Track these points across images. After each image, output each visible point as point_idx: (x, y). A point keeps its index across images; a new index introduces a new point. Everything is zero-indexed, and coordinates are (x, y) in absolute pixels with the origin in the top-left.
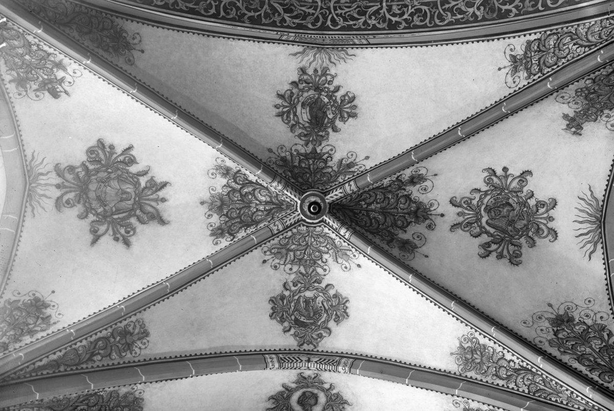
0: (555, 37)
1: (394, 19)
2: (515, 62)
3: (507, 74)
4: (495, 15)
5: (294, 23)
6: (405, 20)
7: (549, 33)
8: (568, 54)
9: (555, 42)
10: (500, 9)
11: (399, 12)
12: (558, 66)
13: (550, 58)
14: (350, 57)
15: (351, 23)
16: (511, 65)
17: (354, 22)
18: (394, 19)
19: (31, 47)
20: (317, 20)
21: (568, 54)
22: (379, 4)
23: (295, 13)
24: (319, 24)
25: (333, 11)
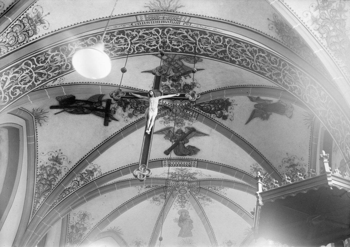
0: (19, 41)
1: (122, 36)
2: (40, 21)
3: (43, 12)
4: (61, 48)
5: (181, 30)
6: (115, 36)
7: (25, 42)
8: (7, 36)
9: (19, 39)
10: (59, 51)
11: (119, 40)
12: (10, 27)
13: (18, 29)
14: (147, 5)
15: (147, 32)
16: (42, 18)
17: (145, 32)
18: (122, 36)
19: (327, 36)
20: (168, 32)
21: (7, 36)
22: (133, 42)
23: (181, 35)
24: (166, 30)
25: (159, 37)
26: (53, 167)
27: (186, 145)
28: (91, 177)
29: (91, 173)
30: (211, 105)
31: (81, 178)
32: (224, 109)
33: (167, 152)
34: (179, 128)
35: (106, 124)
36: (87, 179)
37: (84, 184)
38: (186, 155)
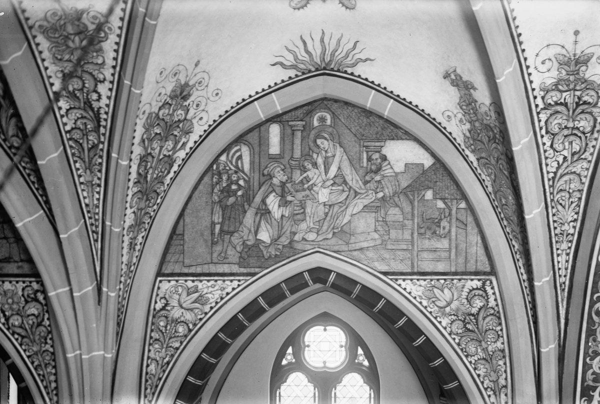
0: (588, 129)
2: (577, 62)
3: (563, 47)
8: (555, 150)
9: (581, 129)
12: (542, 136)
13: (560, 121)
16: (575, 55)
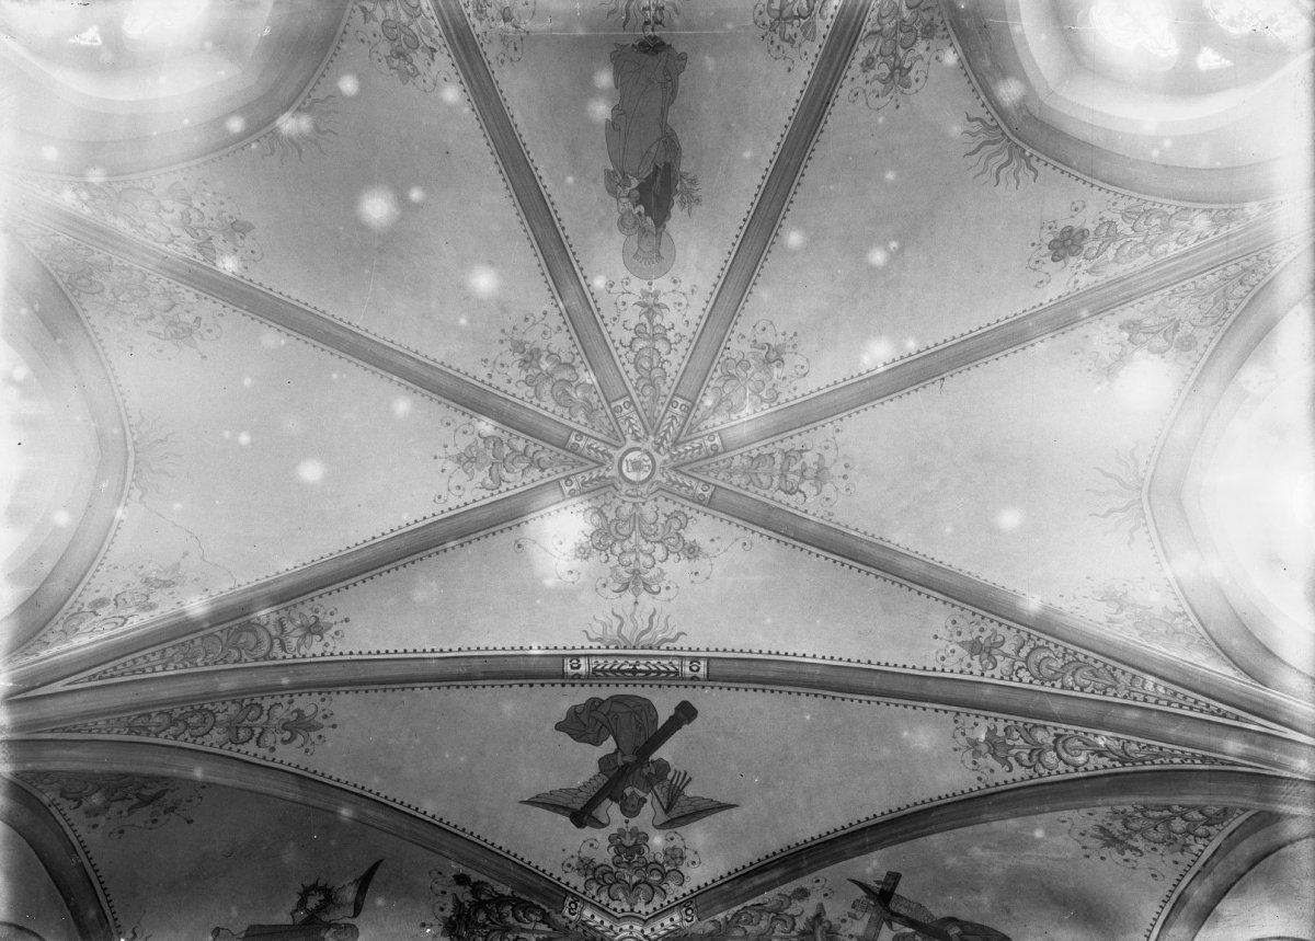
26: (1136, 832)
27: (609, 745)
28: (1000, 733)
29: (995, 746)
30: (511, 920)
31: (1039, 755)
32: (466, 904)
33: (686, 713)
34: (633, 822)
35: (894, 878)
36: (1016, 735)
37: (1035, 726)
38: (615, 699)
